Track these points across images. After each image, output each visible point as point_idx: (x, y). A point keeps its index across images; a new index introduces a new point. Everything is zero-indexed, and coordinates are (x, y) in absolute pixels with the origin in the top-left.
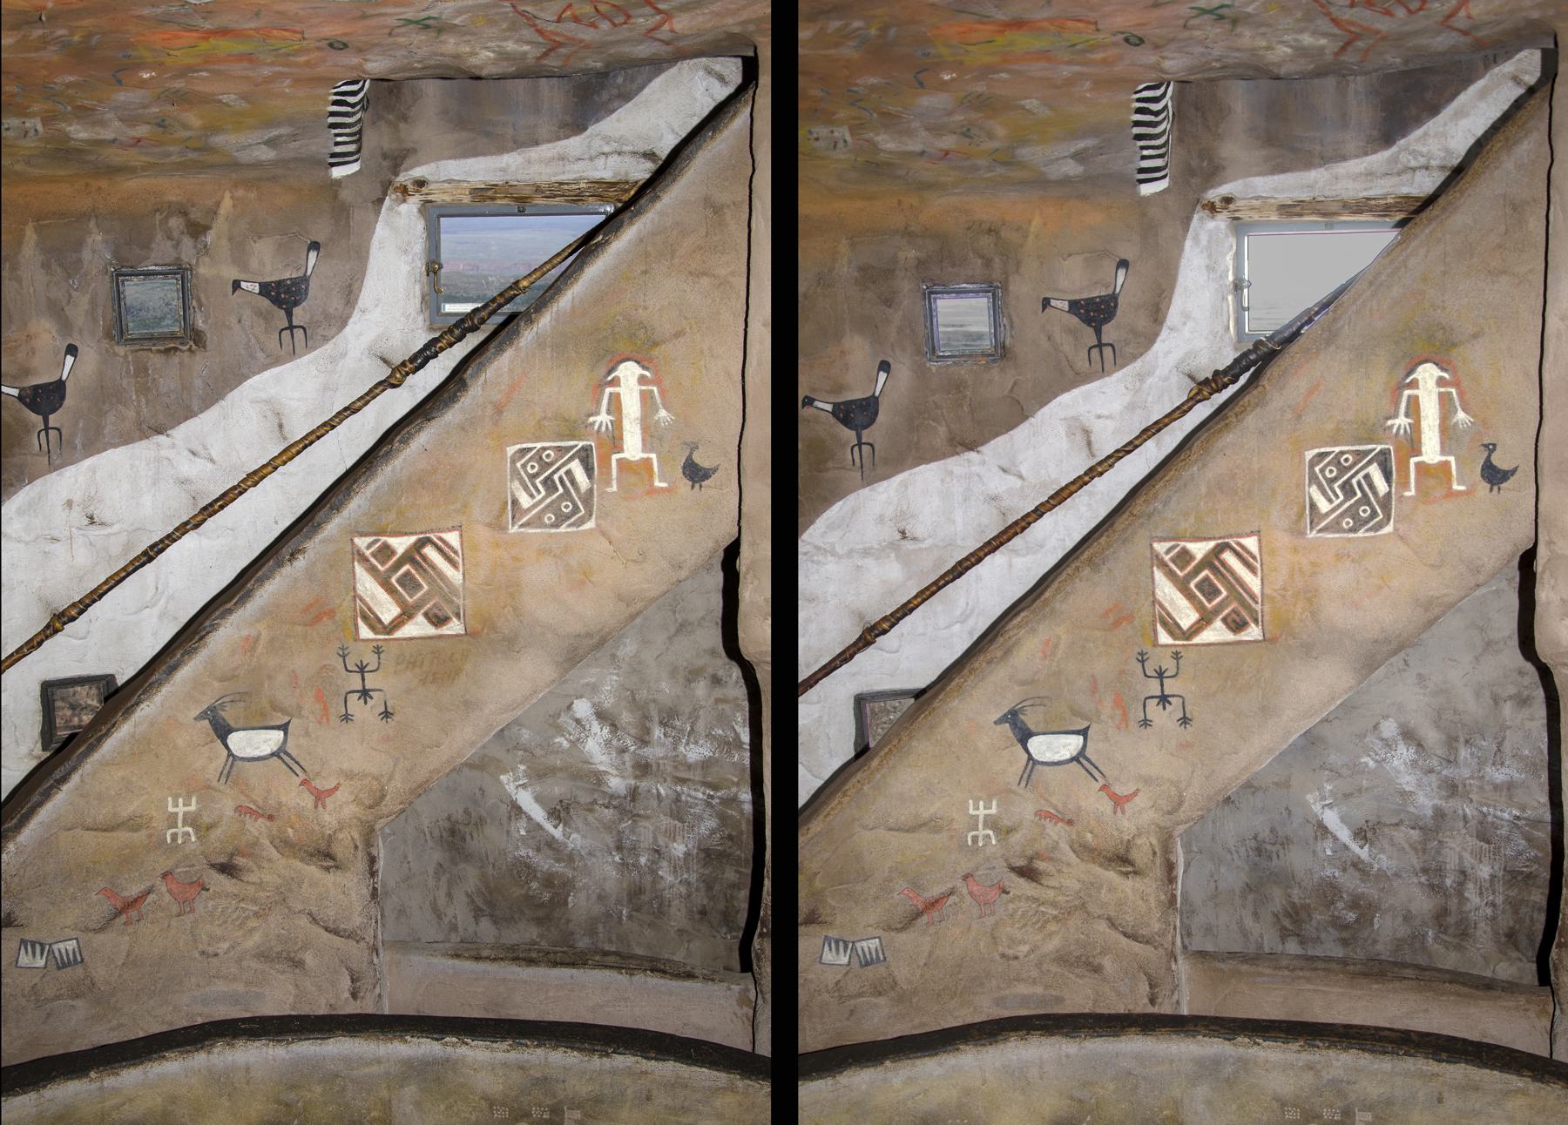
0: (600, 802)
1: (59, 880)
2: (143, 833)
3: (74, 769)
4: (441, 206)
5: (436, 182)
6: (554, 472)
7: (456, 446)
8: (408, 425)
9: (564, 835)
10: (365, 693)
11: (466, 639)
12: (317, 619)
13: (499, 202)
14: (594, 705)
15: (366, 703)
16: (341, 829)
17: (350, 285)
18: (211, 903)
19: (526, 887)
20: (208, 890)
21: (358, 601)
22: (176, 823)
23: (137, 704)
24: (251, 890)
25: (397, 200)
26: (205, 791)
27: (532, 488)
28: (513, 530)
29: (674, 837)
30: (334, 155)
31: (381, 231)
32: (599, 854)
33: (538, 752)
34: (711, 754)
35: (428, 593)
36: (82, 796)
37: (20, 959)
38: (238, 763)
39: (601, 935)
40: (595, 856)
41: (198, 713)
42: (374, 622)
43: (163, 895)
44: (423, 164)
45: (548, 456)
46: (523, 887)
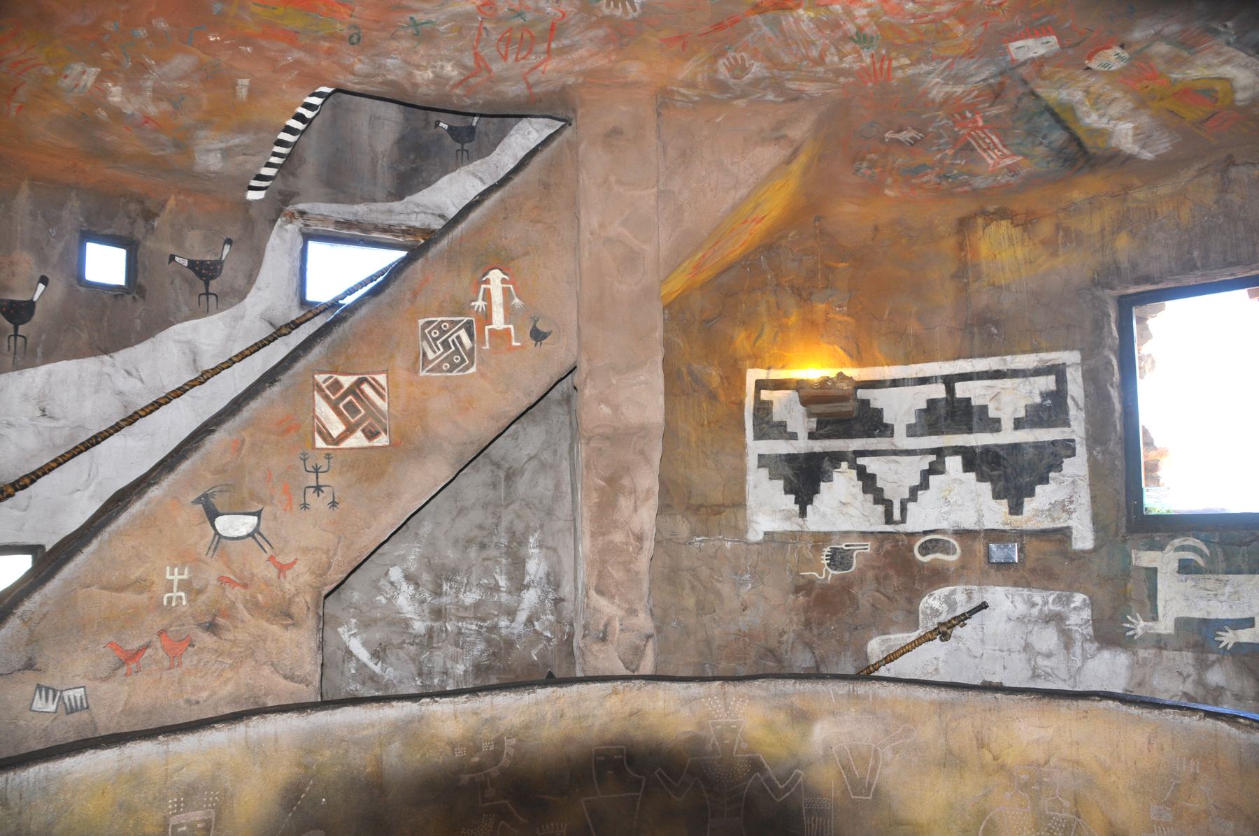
10: (318, 488)
12: (288, 431)
14: (403, 570)
15: (318, 496)
16: (298, 594)
20: (194, 646)
21: (316, 420)
24: (228, 645)
26: (195, 562)
28: (423, 373)
32: (405, 681)
33: (365, 609)
35: (364, 416)
38: (222, 540)
40: (403, 683)
42: (326, 436)
43: (157, 652)
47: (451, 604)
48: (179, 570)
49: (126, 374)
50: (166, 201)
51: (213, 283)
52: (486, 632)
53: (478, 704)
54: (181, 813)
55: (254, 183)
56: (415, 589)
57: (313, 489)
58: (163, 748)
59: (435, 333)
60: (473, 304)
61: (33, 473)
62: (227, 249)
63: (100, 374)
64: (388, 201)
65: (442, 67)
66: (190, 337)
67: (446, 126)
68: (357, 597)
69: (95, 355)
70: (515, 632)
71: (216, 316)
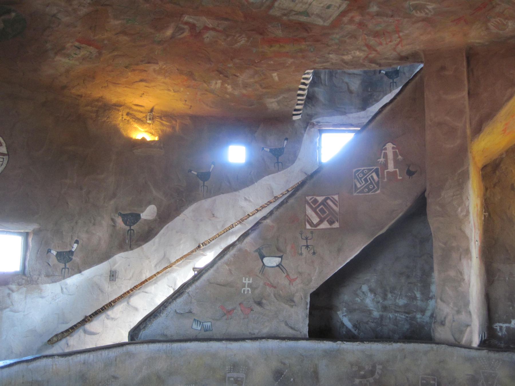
0: (371, 321)
6: (368, 176)
9: (358, 333)
10: (307, 246)
15: (307, 250)
18: (254, 316)
20: (253, 311)
21: (306, 216)
27: (361, 182)
37: (193, 326)
41: (255, 249)
42: (311, 224)
45: (365, 172)
51: (280, 158)
55: (295, 113)
56: (374, 296)
57: (305, 247)
59: (361, 175)
60: (378, 160)
62: (286, 142)
64: (358, 112)
65: (354, 53)
67: (384, 72)
70: (425, 321)
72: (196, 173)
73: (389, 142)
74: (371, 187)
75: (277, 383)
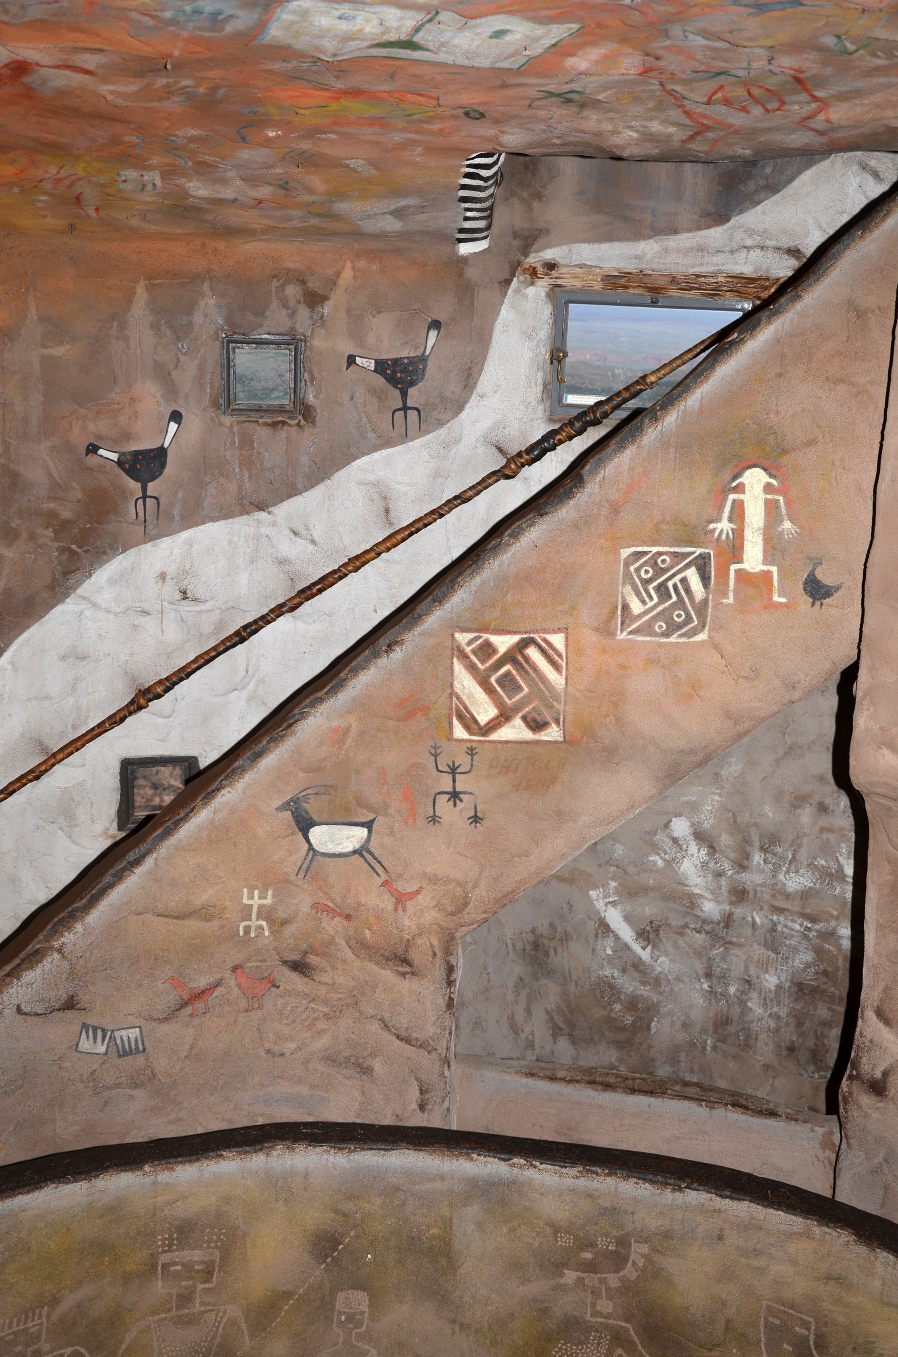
0: (692, 926)
1: (126, 965)
2: (215, 923)
3: (149, 852)
4: (570, 292)
5: (567, 266)
6: (669, 579)
7: (567, 545)
8: (519, 520)
9: (652, 958)
10: (455, 796)
11: (563, 746)
12: (411, 714)
13: (631, 291)
14: (693, 825)
15: (455, 805)
16: (420, 935)
17: (470, 369)
18: (280, 1002)
19: (608, 1009)
20: (278, 987)
21: (454, 699)
22: (250, 915)
23: (218, 790)
24: (323, 990)
25: (524, 282)
26: (283, 885)
27: (644, 594)
28: (622, 636)
29: (767, 968)
30: (462, 231)
31: (506, 313)
33: (631, 869)
34: (812, 885)
35: (527, 696)
36: (155, 880)
37: (80, 1044)
39: (683, 1064)
40: (682, 981)
41: (280, 803)
42: (470, 723)
44: (555, 246)
45: (664, 561)
46: (605, 1008)
47: (763, 885)
48: (260, 892)
49: (292, 536)
50: (338, 274)
51: (412, 391)
52: (818, 937)
53: (595, 1184)
54: (172, 1251)
57: (447, 796)
58: (148, 1180)
59: (647, 572)
60: (712, 526)
61: (167, 679)
62: (433, 335)
63: (257, 538)
66: (381, 474)
68: (620, 852)
69: (248, 513)
71: (418, 442)
72: (114, 457)
73: (754, 466)
74: (678, 617)
75: (323, 1266)
